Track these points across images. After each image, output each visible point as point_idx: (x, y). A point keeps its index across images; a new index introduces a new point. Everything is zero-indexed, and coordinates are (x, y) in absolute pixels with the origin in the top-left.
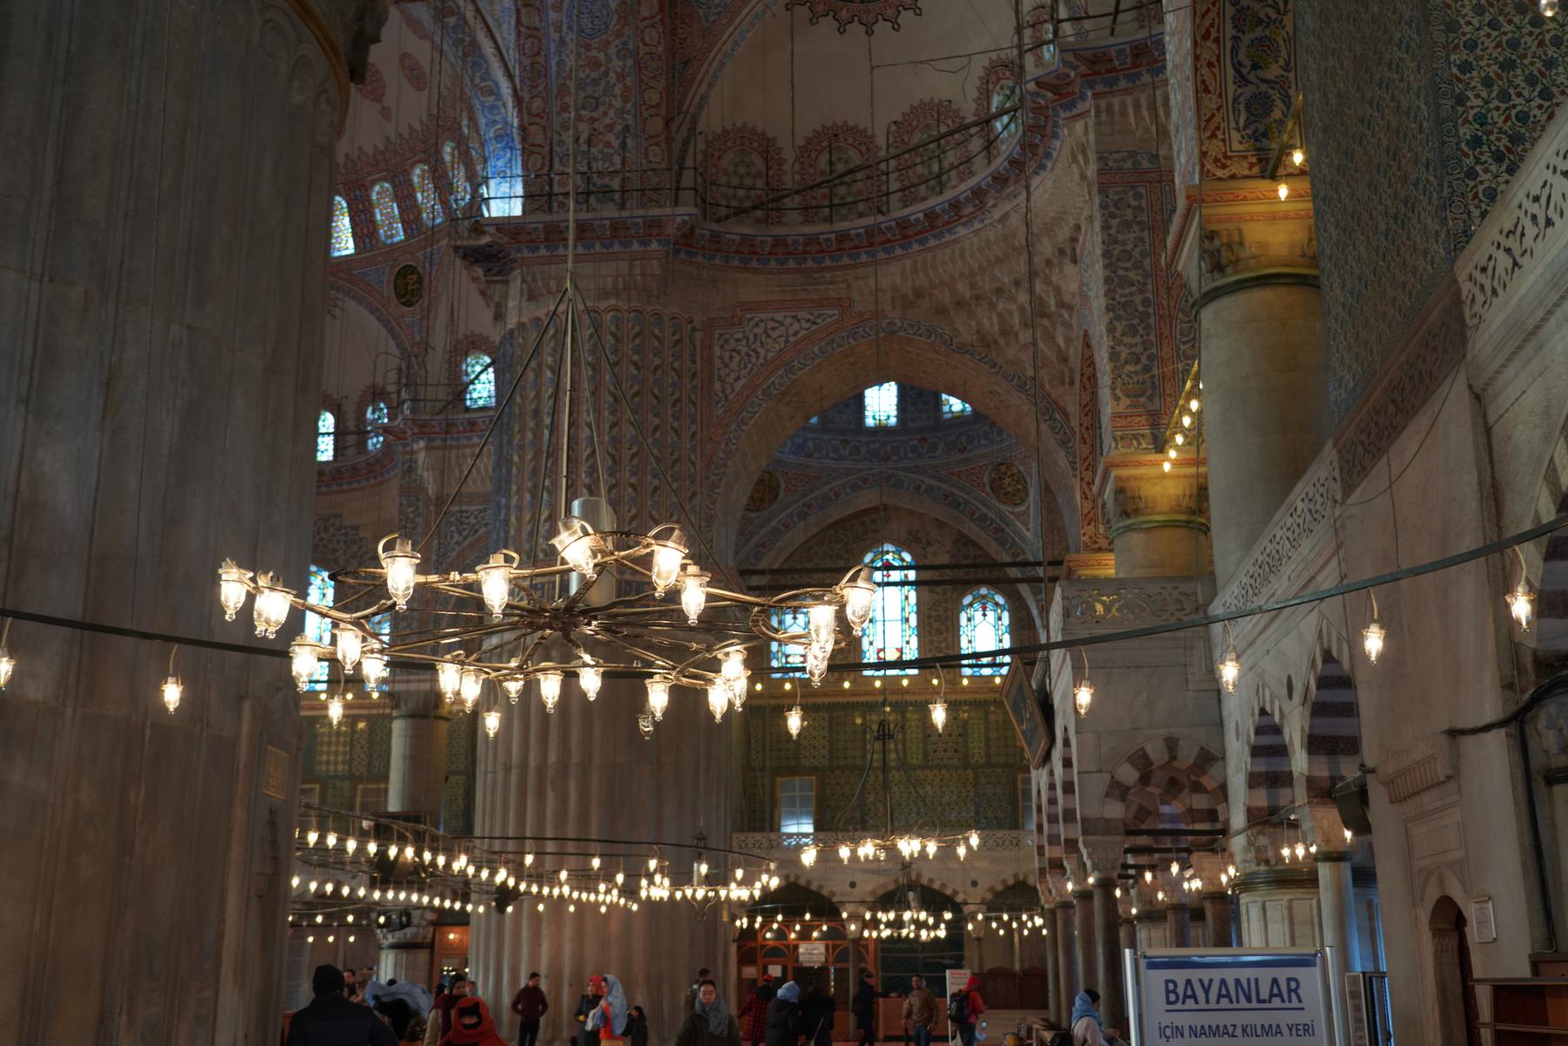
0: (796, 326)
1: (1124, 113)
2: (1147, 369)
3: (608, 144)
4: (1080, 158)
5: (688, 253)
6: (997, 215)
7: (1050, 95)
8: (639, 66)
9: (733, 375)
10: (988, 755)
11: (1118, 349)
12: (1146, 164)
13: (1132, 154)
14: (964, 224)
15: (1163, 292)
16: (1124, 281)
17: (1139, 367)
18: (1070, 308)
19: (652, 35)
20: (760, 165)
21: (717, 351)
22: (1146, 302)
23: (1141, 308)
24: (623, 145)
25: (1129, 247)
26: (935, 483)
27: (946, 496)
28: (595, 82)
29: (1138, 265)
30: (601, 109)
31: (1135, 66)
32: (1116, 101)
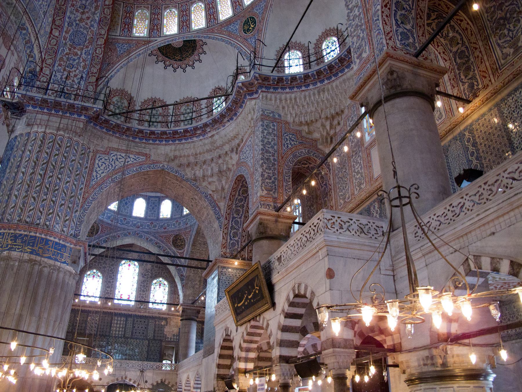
1: (271, 100)
2: (273, 182)
4: (252, 112)
5: (94, 124)
6: (210, 135)
7: (245, 89)
9: (101, 172)
10: (154, 336)
11: (264, 173)
12: (277, 116)
13: (273, 112)
14: (196, 137)
15: (280, 158)
16: (267, 151)
17: (271, 181)
19: (99, 51)
20: (126, 104)
21: (97, 162)
22: (274, 159)
23: (272, 161)
24: (79, 83)
25: (270, 141)
26: (153, 238)
27: (156, 243)
28: (74, 60)
29: (272, 147)
30: (74, 69)
31: (276, 85)
32: (269, 95)
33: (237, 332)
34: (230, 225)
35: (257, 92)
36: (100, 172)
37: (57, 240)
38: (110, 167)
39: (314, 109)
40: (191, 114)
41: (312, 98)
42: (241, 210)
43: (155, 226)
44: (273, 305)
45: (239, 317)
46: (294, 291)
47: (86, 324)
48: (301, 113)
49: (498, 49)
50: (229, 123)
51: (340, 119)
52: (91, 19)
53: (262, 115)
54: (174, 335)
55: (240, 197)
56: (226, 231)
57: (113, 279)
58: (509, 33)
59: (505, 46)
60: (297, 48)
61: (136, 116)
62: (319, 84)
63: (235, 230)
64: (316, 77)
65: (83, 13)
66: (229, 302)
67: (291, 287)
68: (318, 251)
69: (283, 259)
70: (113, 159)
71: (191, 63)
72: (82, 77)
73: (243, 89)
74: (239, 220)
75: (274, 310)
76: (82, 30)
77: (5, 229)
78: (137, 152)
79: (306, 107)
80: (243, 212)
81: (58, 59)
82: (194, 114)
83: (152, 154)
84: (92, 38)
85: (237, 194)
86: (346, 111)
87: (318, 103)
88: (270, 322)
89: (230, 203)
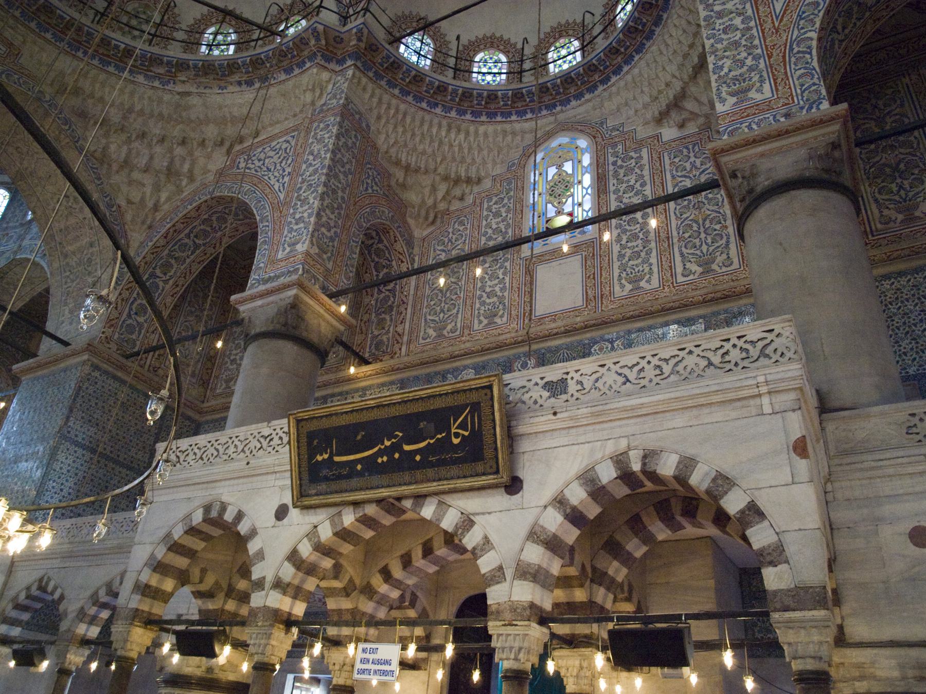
1: (364, 89)
6: (179, 88)
7: (323, 42)
11: (322, 213)
12: (364, 125)
14: (146, 76)
18: (191, 179)
35: (340, 62)
39: (429, 151)
42: (175, 266)
48: (406, 145)
49: (874, 206)
50: (237, 89)
51: (467, 191)
56: (126, 294)
58: (899, 191)
59: (890, 206)
62: (453, 114)
73: (318, 39)
74: (161, 284)
79: (417, 139)
85: (187, 231)
86: (487, 184)
87: (441, 143)
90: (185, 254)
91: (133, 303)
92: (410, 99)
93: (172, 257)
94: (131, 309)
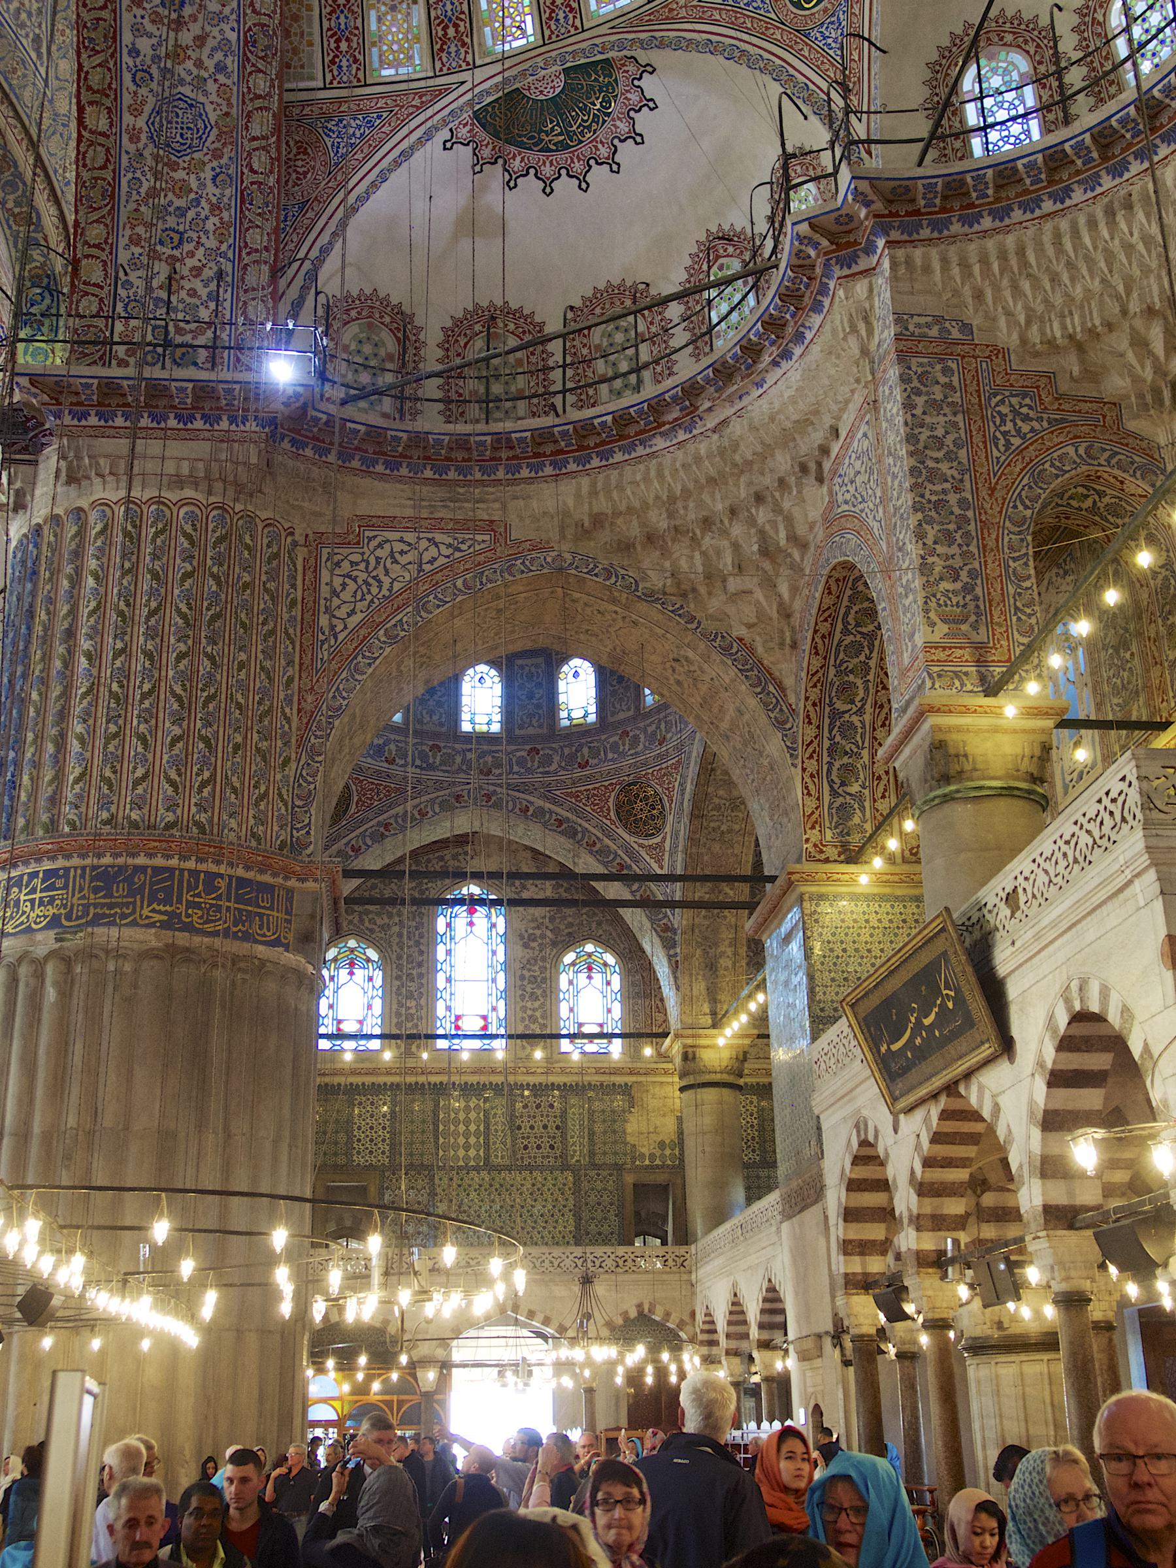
0: (433, 551)
1: (927, 269)
2: (968, 589)
3: (193, 293)
4: (862, 326)
7: (825, 243)
8: (244, 198)
9: (345, 609)
10: (592, 1154)
11: (930, 560)
12: (955, 334)
13: (939, 320)
14: (662, 434)
15: (984, 493)
16: (934, 476)
17: (958, 585)
18: (804, 546)
20: (391, 345)
21: (325, 576)
22: (962, 503)
23: (957, 511)
25: (940, 432)
28: (181, 212)
29: (950, 457)
30: (188, 247)
31: (943, 210)
32: (918, 253)
33: (896, 1131)
34: (827, 744)
36: (342, 613)
37: (240, 872)
38: (374, 590)
39: (1096, 285)
40: (631, 352)
41: (1087, 241)
42: (859, 682)
43: (547, 761)
44: (1007, 1046)
45: (900, 1085)
46: (1068, 1002)
47: (349, 1134)
50: (779, 372)
52: (211, 43)
53: (898, 338)
54: (662, 1145)
55: (849, 639)
56: (812, 766)
57: (420, 965)
60: (1009, 38)
61: (431, 388)
62: (1107, 182)
63: (846, 760)
64: (1095, 155)
65: (179, 24)
66: (860, 1037)
67: (1057, 989)
68: (1130, 882)
69: (1022, 898)
70: (378, 559)
71: (604, 152)
72: (220, 275)
73: (816, 245)
74: (855, 719)
75: (1012, 1059)
76: (187, 90)
77: (68, 857)
78: (456, 521)
80: (867, 690)
81: (123, 218)
82: (644, 348)
83: (513, 519)
84: (227, 114)
87: (1110, 257)
88: (1001, 1100)
89: (816, 663)
90: (862, 658)
91: (829, 771)
92: (1017, 215)
93: (847, 672)
94: (831, 783)
